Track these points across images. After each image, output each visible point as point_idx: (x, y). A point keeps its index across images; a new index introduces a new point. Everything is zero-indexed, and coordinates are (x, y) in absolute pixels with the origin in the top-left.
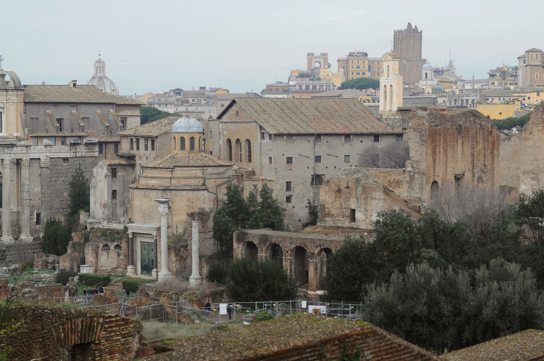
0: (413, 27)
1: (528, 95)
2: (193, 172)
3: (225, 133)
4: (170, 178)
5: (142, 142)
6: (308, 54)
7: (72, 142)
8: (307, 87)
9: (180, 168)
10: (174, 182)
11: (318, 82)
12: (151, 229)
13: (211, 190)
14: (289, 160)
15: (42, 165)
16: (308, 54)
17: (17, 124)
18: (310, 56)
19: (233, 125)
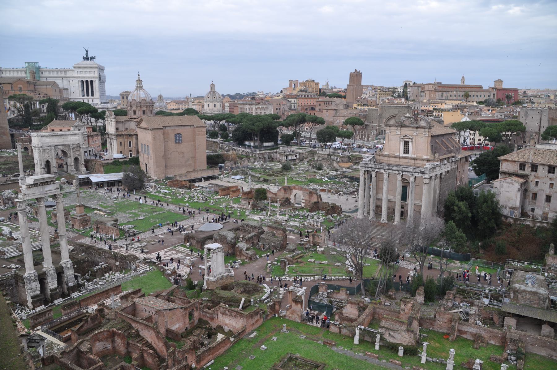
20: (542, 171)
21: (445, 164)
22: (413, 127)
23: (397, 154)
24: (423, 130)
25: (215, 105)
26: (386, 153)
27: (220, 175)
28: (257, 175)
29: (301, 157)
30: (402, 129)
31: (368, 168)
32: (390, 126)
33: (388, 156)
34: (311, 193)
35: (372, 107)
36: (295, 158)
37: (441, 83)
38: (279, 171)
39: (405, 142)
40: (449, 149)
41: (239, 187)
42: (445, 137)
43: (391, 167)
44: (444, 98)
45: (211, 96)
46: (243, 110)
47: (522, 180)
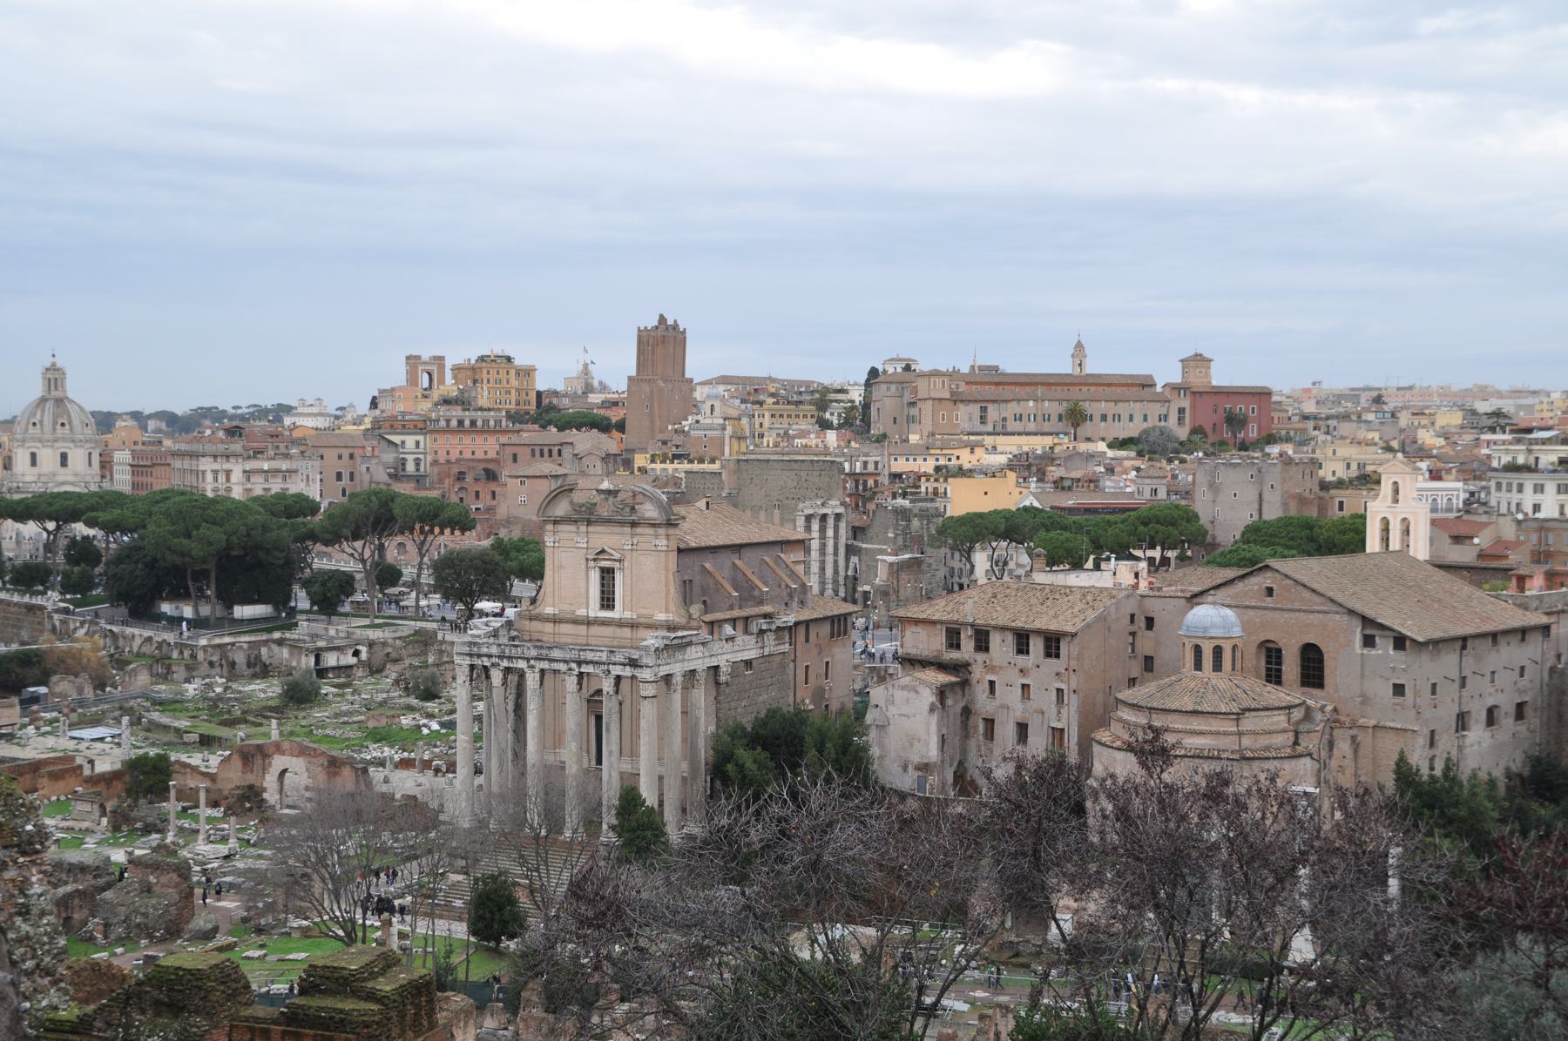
0: (670, 322)
1: (957, 453)
2: (1276, 719)
5: (995, 640)
6: (408, 358)
16: (408, 358)
18: (413, 360)
20: (1002, 647)
21: (731, 639)
22: (621, 523)
23: (581, 612)
24: (651, 531)
25: (64, 457)
26: (549, 610)
27: (24, 726)
28: (176, 724)
29: (380, 654)
30: (591, 529)
31: (479, 656)
32: (556, 522)
33: (555, 620)
34: (334, 765)
36: (354, 661)
37: (996, 368)
38: (271, 709)
39: (603, 570)
40: (756, 593)
41: (79, 761)
42: (747, 553)
43: (544, 652)
45: (48, 419)
46: (190, 480)
47: (944, 678)
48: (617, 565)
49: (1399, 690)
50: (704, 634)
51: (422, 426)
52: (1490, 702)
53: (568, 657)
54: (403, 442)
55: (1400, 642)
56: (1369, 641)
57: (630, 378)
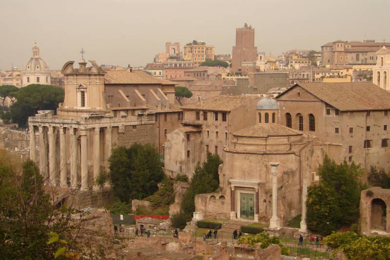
0: (249, 26)
1: (341, 71)
2: (282, 140)
3: (284, 108)
4: (266, 145)
5: (209, 115)
6: (167, 43)
7: (140, 113)
8: (176, 65)
9: (272, 137)
10: (268, 148)
11: (182, 62)
12: (253, 184)
13: (297, 154)
14: (351, 130)
15: (120, 131)
16: (167, 43)
17: (100, 101)
19: (294, 103)
22: (86, 75)
23: (75, 108)
30: (78, 77)
31: (35, 122)
33: (68, 111)
35: (243, 77)
39: (81, 92)
44: (360, 62)
45: (33, 66)
48: (85, 90)
49: (337, 130)
50: (112, 114)
51: (162, 67)
52: (384, 137)
53: (60, 122)
54: (155, 73)
55: (337, 112)
56: (328, 113)
57: (234, 47)
